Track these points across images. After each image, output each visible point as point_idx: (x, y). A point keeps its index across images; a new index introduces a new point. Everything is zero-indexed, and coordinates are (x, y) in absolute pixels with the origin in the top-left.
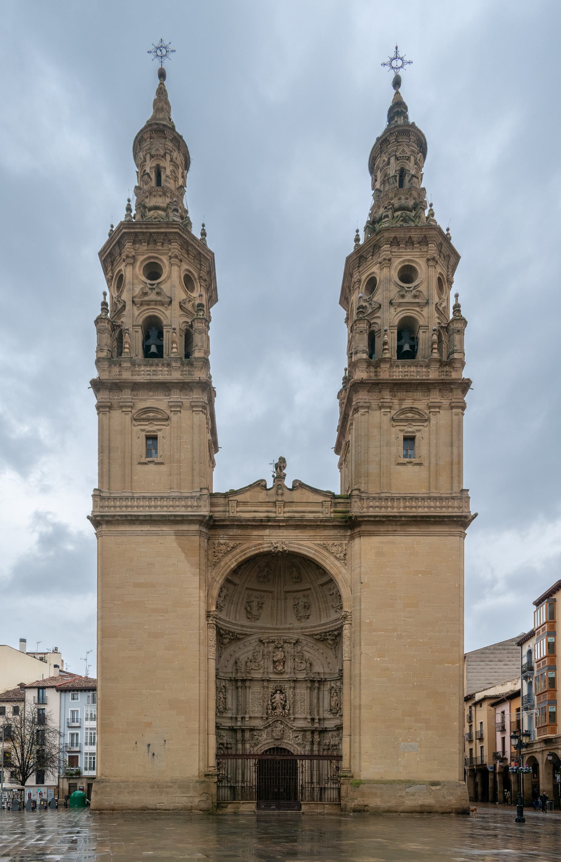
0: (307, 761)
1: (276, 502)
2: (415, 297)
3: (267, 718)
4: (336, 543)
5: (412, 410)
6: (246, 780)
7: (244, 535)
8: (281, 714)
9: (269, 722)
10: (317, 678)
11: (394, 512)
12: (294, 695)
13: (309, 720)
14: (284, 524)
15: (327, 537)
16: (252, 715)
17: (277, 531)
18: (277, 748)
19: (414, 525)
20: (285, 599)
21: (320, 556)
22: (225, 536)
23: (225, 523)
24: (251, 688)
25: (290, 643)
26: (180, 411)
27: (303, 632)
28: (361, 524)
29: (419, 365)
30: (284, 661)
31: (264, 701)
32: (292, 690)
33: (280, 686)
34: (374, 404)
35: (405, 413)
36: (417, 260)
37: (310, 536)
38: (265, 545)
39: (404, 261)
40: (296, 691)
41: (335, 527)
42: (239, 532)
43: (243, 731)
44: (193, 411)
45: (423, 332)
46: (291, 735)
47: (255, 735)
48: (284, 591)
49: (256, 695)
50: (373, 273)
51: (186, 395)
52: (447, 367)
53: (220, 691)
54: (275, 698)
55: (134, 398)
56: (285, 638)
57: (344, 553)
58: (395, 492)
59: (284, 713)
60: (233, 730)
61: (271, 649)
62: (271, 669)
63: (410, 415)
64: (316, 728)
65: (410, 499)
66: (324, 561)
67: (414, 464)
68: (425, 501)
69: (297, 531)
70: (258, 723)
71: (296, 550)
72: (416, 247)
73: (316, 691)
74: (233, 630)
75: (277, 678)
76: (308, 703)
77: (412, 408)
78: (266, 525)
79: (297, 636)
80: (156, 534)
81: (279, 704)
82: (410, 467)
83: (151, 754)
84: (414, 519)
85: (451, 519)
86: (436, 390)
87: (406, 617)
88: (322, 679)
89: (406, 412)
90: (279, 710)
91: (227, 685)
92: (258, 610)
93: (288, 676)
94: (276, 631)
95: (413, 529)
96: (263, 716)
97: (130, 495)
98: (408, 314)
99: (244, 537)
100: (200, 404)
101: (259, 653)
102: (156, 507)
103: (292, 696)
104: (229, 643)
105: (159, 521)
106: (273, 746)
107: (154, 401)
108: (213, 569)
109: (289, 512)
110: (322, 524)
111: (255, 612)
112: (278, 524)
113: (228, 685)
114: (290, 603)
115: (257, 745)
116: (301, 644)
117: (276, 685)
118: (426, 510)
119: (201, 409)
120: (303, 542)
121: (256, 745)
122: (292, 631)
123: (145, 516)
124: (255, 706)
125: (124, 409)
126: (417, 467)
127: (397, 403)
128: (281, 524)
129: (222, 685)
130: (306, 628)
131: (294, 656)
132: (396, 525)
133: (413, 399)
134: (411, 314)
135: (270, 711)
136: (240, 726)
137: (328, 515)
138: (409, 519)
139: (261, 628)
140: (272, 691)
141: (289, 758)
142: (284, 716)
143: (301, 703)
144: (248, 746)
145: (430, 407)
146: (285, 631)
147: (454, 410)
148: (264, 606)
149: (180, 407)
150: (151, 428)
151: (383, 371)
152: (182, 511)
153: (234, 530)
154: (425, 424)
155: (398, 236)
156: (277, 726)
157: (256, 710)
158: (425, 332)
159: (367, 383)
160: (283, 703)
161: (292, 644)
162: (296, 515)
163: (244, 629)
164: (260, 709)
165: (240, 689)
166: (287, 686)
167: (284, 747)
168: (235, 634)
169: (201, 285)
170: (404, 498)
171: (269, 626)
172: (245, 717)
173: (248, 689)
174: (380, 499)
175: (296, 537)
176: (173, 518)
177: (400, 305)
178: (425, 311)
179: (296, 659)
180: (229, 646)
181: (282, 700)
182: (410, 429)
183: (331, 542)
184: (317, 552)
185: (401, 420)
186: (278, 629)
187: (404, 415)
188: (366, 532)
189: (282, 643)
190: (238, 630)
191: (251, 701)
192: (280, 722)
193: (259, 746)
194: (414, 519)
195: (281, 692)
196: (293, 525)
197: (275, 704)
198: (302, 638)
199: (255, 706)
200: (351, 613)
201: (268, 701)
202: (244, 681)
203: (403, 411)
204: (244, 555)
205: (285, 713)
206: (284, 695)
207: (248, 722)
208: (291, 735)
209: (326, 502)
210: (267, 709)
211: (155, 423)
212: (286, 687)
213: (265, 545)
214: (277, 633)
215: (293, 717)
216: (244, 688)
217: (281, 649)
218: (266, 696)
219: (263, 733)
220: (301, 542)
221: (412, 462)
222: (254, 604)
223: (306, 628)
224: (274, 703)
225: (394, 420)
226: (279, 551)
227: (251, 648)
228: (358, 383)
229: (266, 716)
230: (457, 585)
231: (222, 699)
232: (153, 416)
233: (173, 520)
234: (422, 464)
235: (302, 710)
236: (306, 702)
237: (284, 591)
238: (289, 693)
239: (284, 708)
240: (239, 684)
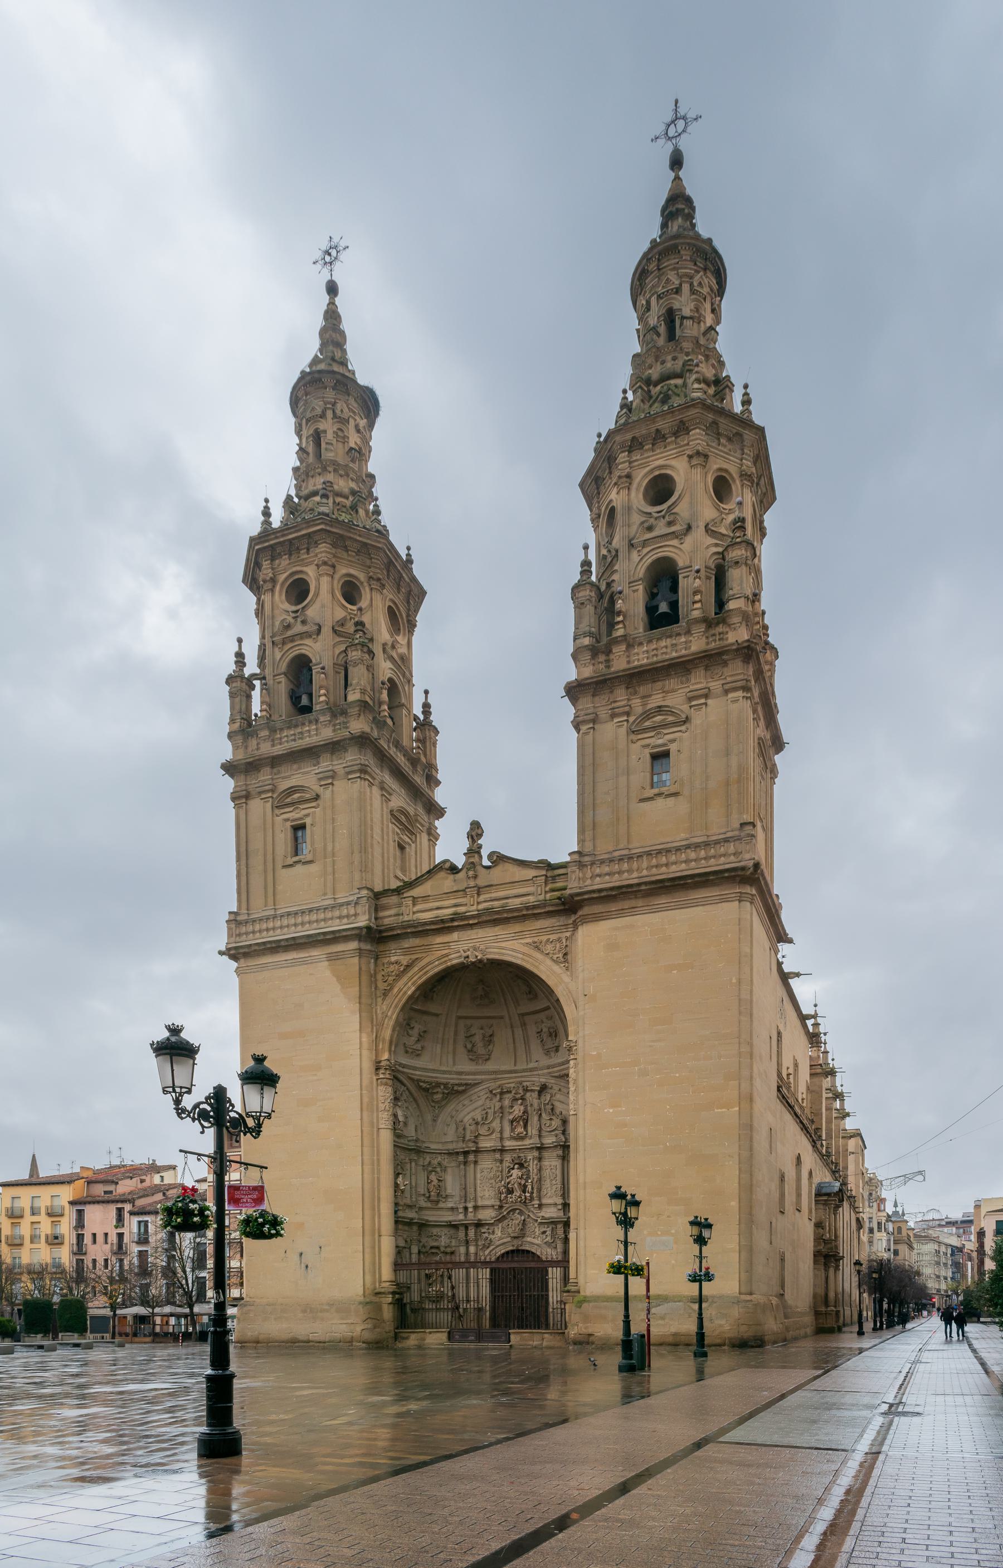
0: (559, 1269)
1: (467, 890)
2: (670, 524)
3: (501, 1207)
4: (552, 937)
6: (472, 1299)
11: (633, 878)
12: (540, 1170)
13: (560, 1207)
14: (476, 921)
16: (480, 1203)
17: (469, 932)
18: (518, 1251)
20: (524, 1025)
24: (480, 1163)
25: (532, 1091)
26: (332, 784)
27: (550, 1073)
29: (674, 634)
30: (524, 1119)
34: (603, 713)
36: (673, 463)
41: (550, 914)
43: (466, 1227)
44: (349, 779)
46: (537, 1230)
47: (484, 1233)
48: (519, 1014)
50: (611, 501)
51: (341, 758)
52: (721, 626)
53: (431, 1171)
54: (511, 1176)
55: (275, 777)
56: (525, 1084)
57: (564, 951)
58: (637, 846)
60: (454, 1226)
61: (507, 1103)
62: (507, 1133)
63: (659, 718)
66: (537, 967)
68: (681, 854)
69: (497, 928)
70: (487, 1215)
71: (497, 957)
72: (669, 443)
74: (445, 1081)
79: (544, 1080)
80: (304, 962)
81: (516, 1185)
83: (303, 1266)
84: (661, 885)
87: (653, 1041)
90: (517, 1193)
91: (445, 1163)
92: (485, 1046)
93: (531, 1141)
94: (514, 1075)
95: (662, 900)
97: (272, 912)
98: (659, 555)
100: (356, 768)
101: (489, 1111)
102: (303, 924)
103: (535, 1171)
104: (443, 1099)
105: (305, 943)
106: (511, 1248)
107: (300, 775)
108: (384, 1000)
110: (530, 912)
111: (480, 1050)
113: (446, 1161)
114: (532, 1030)
115: (488, 1247)
116: (550, 1091)
118: (683, 866)
119: (358, 775)
120: (507, 943)
121: (485, 1247)
122: (535, 1073)
123: (287, 940)
125: (263, 796)
128: (471, 922)
129: (435, 1162)
130: (554, 1066)
131: (540, 1109)
132: (636, 898)
135: (503, 1196)
137: (542, 897)
138: (653, 886)
139: (495, 1072)
141: (532, 1265)
142: (525, 1202)
143: (551, 1180)
144: (472, 1249)
146: (526, 1074)
147: (731, 695)
148: (495, 1039)
149: (333, 777)
150: (295, 815)
152: (335, 926)
154: (683, 728)
155: (637, 435)
156: (513, 1217)
159: (588, 684)
161: (537, 1093)
162: (496, 904)
163: (463, 1077)
164: (492, 1193)
166: (530, 1157)
167: (527, 1248)
168: (450, 1086)
169: (371, 589)
170: (649, 854)
171: (504, 1068)
176: (321, 937)
177: (645, 543)
178: (689, 540)
179: (544, 1115)
180: (447, 1104)
182: (658, 741)
183: (544, 938)
186: (515, 1072)
187: (651, 720)
189: (521, 1091)
190: (453, 1079)
191: (478, 1182)
192: (518, 1211)
193: (491, 1248)
194: (661, 885)
195: (521, 1166)
197: (510, 1186)
198: (552, 1081)
200: (576, 1042)
202: (466, 1153)
207: (472, 1214)
208: (537, 1230)
211: (302, 807)
212: (529, 1158)
214: (516, 1077)
215: (538, 1202)
217: (520, 1102)
219: (496, 1229)
220: (503, 944)
222: (477, 1039)
223: (554, 1066)
224: (508, 1183)
227: (480, 1103)
229: (498, 1203)
230: (734, 981)
231: (435, 1182)
232: (299, 798)
233: (322, 940)
235: (553, 1191)
237: (519, 1014)
238: (533, 1167)
239: (524, 1192)
240: (461, 1158)
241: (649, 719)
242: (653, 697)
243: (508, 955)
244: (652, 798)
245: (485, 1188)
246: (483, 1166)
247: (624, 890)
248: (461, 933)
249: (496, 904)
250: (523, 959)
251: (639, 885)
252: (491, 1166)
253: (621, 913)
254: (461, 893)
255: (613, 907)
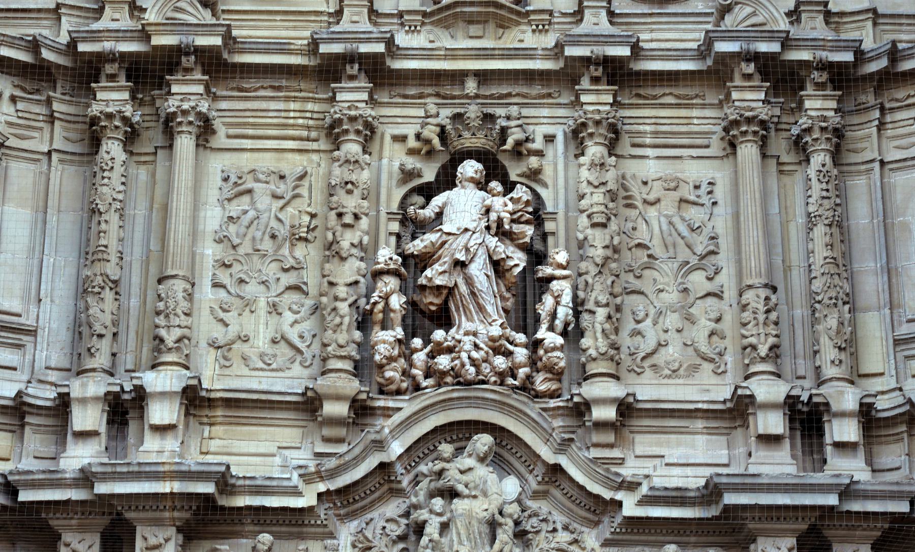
8: (500, 362)
9: (380, 445)
10: (814, 44)
24: (220, 139)
31: (333, 252)
32: (595, 150)
33: (489, 118)
40: (632, 168)
49: (264, 201)
59: (521, 354)
64: (847, 491)
73: (819, 159)
75: (451, 54)
76: (755, 261)
81: (479, 270)
88: (860, 55)
96: (324, 384)
117: (446, 112)
124: (248, 305)
136: (86, 478)
140: (411, 163)
142: (526, 388)
143: (686, 268)
156: (453, 476)
157: (261, 341)
160: (518, 260)
165: (112, 149)
172: (141, 396)
173: (185, 143)
181: (502, 233)
191: (210, 251)
192: (483, 441)
197: (434, 274)
199: (248, 305)
201: (367, 251)
205: (533, 362)
206: (521, 192)
207: (171, 444)
210: (364, 322)
212: (539, 132)
216: (153, 137)
218: (351, 203)
224: (424, 260)
229: (352, 386)
235: (700, 333)
236: (724, 259)
245: (252, 289)
246: (246, 161)
252: (293, 164)
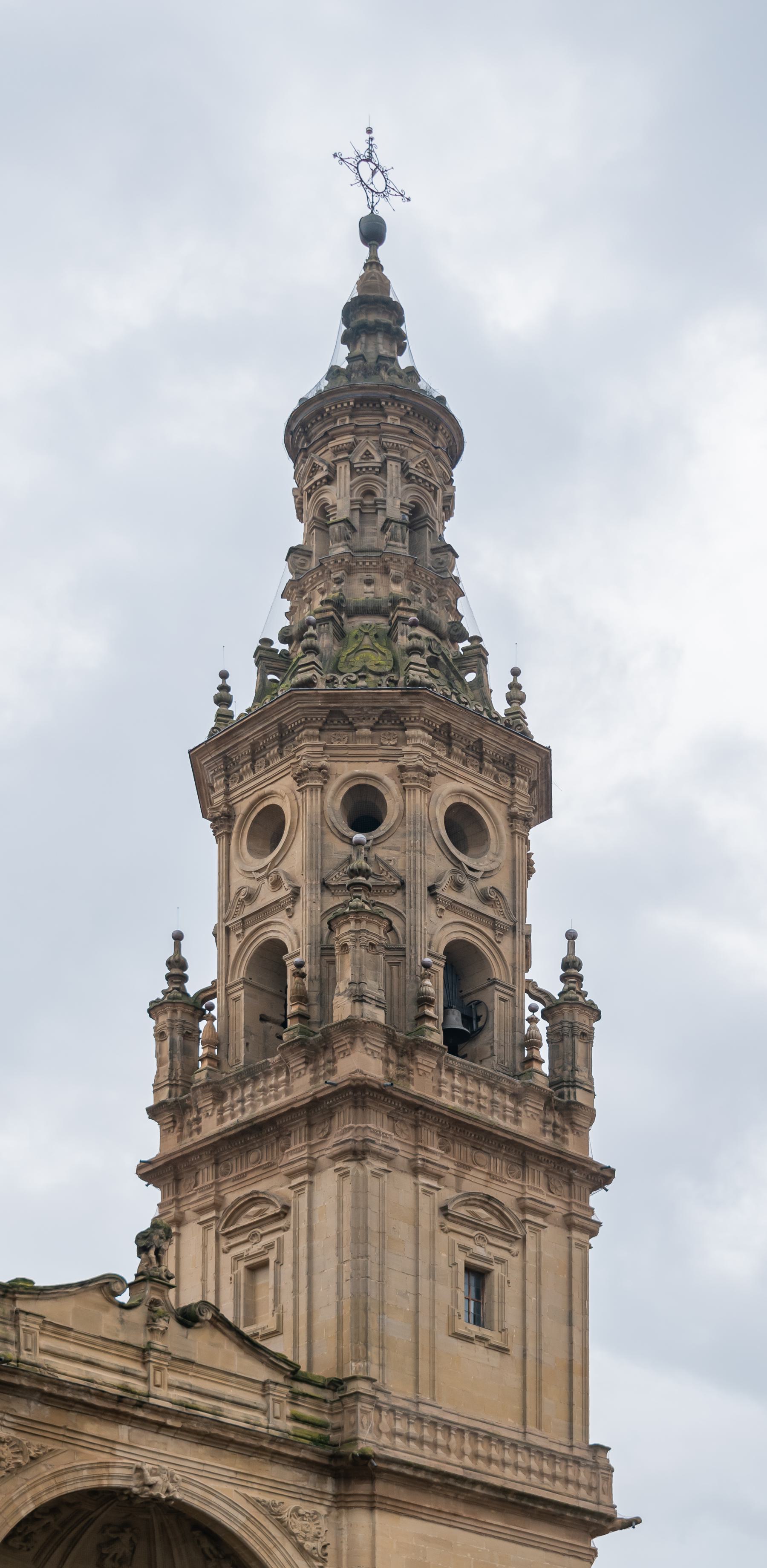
4: (305, 1509)
5: (488, 1201)
7: (65, 1428)
14: (178, 1424)
15: (277, 1486)
17: (151, 1436)
19: (494, 1509)
21: (259, 1534)
22: (7, 1417)
23: (16, 1381)
28: (377, 1475)
35: (471, 1205)
37: (236, 1472)
38: (117, 1471)
39: (461, 792)
41: (299, 1463)
42: (45, 1413)
45: (501, 999)
65: (485, 1437)
67: (491, 1345)
69: (202, 1450)
71: (196, 1503)
77: (490, 1198)
78: (126, 1415)
82: (479, 1349)
84: (502, 1496)
85: (579, 1517)
86: (540, 1168)
89: (472, 1202)
95: (494, 1520)
99: (61, 1432)
109: (179, 1388)
110: (274, 1447)
112: (160, 1419)
120: (224, 1486)
126: (495, 1356)
127: (453, 1172)
128: (169, 1422)
132: (455, 1498)
133: (488, 1174)
134: (475, 941)
138: (492, 1494)
145: (524, 1209)
151: (421, 1073)
153: (32, 1404)
158: (505, 1001)
170: (474, 1433)
174: (420, 1419)
175: (201, 1467)
183: (292, 1504)
184: (253, 1524)
185: (462, 1221)
188: (389, 1502)
194: (502, 1496)
196: (197, 1433)
203: (470, 1199)
204: (59, 1486)
209: (278, 1388)
213: (117, 1471)
220: (212, 1484)
221: (487, 1340)
225: (446, 1215)
226: (156, 1499)
228: (373, 1089)
234: (508, 1350)
241: (466, 1205)
242: (472, 1173)
243: (219, 1507)
244: (472, 1339)
247: (451, 1481)
248: (135, 1431)
249: (201, 1402)
250: (244, 1526)
251: (475, 1483)
253: (435, 1516)
254: (133, 1351)
255: (428, 1502)
